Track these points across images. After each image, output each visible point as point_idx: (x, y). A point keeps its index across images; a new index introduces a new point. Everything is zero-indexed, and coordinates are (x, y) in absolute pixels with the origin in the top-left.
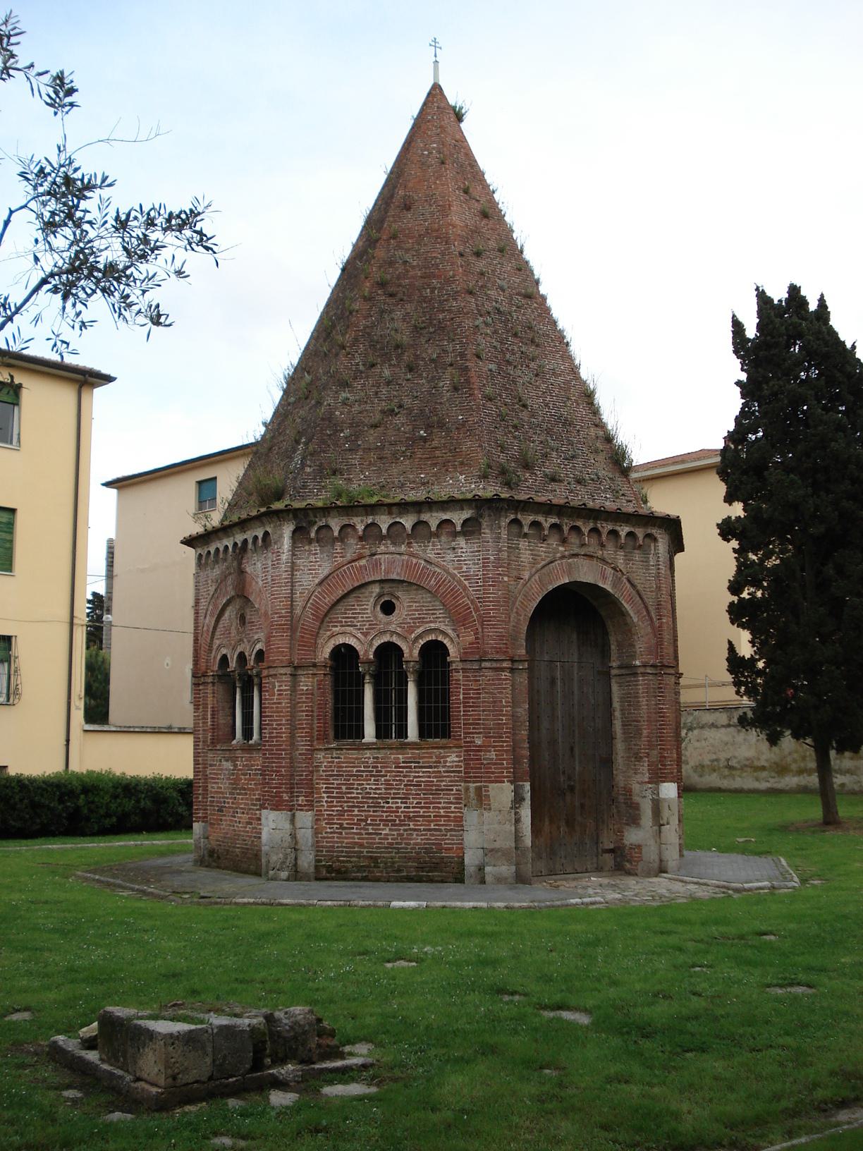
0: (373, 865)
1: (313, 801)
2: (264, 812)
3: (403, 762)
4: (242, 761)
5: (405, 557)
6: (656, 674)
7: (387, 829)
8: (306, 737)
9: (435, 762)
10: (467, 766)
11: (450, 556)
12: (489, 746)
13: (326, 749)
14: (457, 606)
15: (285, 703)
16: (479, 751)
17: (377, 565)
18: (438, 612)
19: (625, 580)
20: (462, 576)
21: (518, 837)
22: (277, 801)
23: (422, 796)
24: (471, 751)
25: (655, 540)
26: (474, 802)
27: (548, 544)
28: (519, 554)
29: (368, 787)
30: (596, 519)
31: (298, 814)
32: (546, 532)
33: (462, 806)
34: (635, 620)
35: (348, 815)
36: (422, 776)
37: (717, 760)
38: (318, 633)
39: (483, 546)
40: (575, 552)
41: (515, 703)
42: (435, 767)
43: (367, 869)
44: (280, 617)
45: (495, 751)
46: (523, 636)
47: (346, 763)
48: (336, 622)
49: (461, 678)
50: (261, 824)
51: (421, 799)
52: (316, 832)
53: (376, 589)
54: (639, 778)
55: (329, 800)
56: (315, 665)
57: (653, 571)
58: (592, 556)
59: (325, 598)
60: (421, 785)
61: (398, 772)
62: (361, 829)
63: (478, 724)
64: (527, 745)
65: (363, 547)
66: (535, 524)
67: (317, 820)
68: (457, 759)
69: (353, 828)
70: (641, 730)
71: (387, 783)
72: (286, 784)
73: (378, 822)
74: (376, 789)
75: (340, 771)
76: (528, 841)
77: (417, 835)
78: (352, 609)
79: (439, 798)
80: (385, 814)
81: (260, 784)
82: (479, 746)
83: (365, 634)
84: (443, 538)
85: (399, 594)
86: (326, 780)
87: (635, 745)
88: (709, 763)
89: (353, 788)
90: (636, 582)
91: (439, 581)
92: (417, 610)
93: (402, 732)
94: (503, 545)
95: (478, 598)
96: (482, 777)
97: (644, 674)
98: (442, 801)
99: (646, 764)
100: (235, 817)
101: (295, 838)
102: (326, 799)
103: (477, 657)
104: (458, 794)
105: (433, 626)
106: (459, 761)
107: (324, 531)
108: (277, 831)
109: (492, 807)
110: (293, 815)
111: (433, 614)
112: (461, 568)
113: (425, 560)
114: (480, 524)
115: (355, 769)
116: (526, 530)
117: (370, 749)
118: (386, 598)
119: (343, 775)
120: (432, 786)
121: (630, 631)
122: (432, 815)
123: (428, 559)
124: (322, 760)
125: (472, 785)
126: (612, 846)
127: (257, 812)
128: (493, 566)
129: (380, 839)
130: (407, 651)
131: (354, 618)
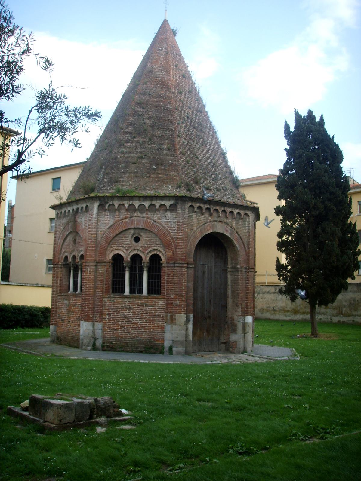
0: (126, 345)
1: (102, 318)
2: (82, 322)
4: (72, 300)
5: (145, 219)
7: (133, 331)
9: (154, 304)
10: (167, 306)
11: (164, 219)
12: (177, 299)
13: (109, 297)
15: (92, 277)
16: (172, 300)
17: (133, 221)
18: (158, 242)
19: (235, 232)
21: (187, 336)
22: (87, 318)
23: (148, 318)
25: (248, 216)
26: (169, 321)
28: (193, 219)
29: (125, 313)
30: (225, 206)
31: (96, 323)
32: (204, 211)
34: (239, 249)
36: (148, 310)
37: (269, 307)
38: (107, 249)
39: (178, 216)
41: (188, 281)
42: (154, 306)
46: (193, 253)
47: (116, 303)
49: (166, 270)
50: (80, 327)
51: (147, 319)
52: (103, 331)
53: (132, 232)
54: (237, 314)
56: (105, 262)
58: (222, 222)
59: (110, 234)
61: (139, 308)
62: (122, 330)
63: (173, 289)
64: (192, 299)
65: (127, 214)
66: (200, 208)
68: (163, 303)
70: (239, 294)
71: (134, 312)
72: (91, 311)
73: (129, 328)
76: (191, 338)
78: (121, 240)
80: (132, 325)
81: (80, 310)
82: (172, 298)
83: (127, 250)
84: (161, 212)
85: (142, 234)
86: (108, 310)
87: (236, 300)
88: (266, 308)
89: (119, 314)
90: (240, 233)
92: (149, 241)
93: (141, 291)
94: (186, 215)
95: (175, 237)
96: (173, 311)
97: (241, 271)
99: (240, 308)
100: (68, 323)
102: (108, 318)
103: (173, 262)
105: (155, 248)
106: (164, 304)
107: (111, 206)
108: (87, 330)
111: (156, 243)
112: (168, 224)
113: (153, 220)
114: (177, 206)
115: (120, 306)
116: (196, 210)
118: (136, 235)
119: (115, 308)
121: (236, 253)
122: (152, 326)
123: (154, 220)
124: (107, 302)
125: (169, 314)
126: (224, 341)
127: (79, 322)
128: (182, 224)
129: (130, 335)
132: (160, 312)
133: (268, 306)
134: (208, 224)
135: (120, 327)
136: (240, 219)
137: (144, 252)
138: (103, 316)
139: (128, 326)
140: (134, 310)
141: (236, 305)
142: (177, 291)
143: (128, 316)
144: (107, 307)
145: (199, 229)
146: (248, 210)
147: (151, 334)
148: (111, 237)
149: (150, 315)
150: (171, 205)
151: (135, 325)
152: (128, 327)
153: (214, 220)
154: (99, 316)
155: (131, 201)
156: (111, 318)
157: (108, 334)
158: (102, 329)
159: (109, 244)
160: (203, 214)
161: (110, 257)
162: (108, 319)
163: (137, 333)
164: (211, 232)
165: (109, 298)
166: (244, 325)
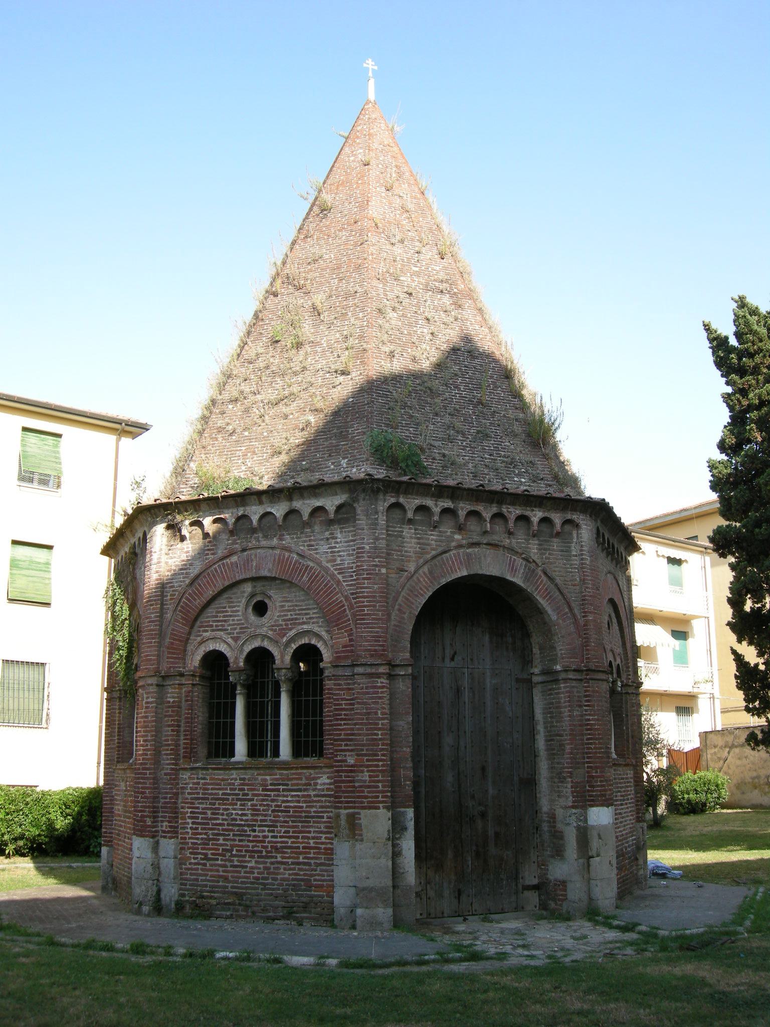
0: (237, 902)
1: (177, 827)
3: (271, 784)
5: (277, 552)
6: (581, 680)
8: (171, 754)
9: (306, 784)
11: (324, 548)
12: (361, 766)
13: (192, 769)
14: (330, 604)
16: (351, 771)
17: (248, 561)
18: (311, 612)
19: (540, 573)
20: (336, 570)
21: (396, 872)
22: (142, 826)
23: (290, 823)
24: (342, 771)
25: (577, 526)
26: (346, 832)
27: (440, 532)
28: (403, 542)
29: (234, 812)
30: (500, 503)
31: (163, 842)
32: (436, 518)
33: (332, 835)
34: (554, 617)
35: (213, 844)
36: (290, 800)
37: (758, 777)
38: (188, 639)
40: (474, 541)
41: (393, 714)
42: (305, 790)
43: (231, 907)
44: (150, 622)
45: (368, 771)
46: (407, 637)
47: (212, 784)
48: (207, 626)
51: (288, 827)
52: (181, 862)
54: (562, 802)
55: (194, 826)
56: (182, 675)
57: (576, 561)
59: (195, 600)
60: (289, 812)
61: (266, 795)
62: (225, 860)
65: (234, 543)
67: (182, 849)
68: (328, 781)
69: (217, 859)
70: (563, 745)
71: (254, 809)
72: (149, 807)
73: (243, 853)
74: (242, 815)
75: (205, 794)
77: (285, 869)
78: (223, 612)
79: (307, 827)
80: (251, 844)
82: (352, 766)
83: (236, 639)
84: (317, 528)
85: (271, 593)
87: (558, 763)
88: (751, 780)
89: (218, 814)
90: (554, 575)
91: (312, 576)
92: (289, 611)
94: (381, 533)
95: (352, 594)
96: (355, 802)
97: (566, 680)
98: (312, 830)
99: (569, 785)
101: (159, 868)
102: (191, 825)
103: (349, 662)
104: (329, 822)
105: (305, 627)
106: (330, 784)
108: (141, 860)
109: (365, 838)
110: (157, 843)
111: (306, 614)
112: (335, 561)
113: (298, 554)
114: (354, 509)
115: (221, 792)
116: (410, 515)
117: (236, 769)
118: (259, 598)
119: (208, 799)
120: (301, 812)
121: (550, 631)
122: (301, 846)
123: (300, 552)
124: (188, 781)
125: (344, 812)
126: (535, 881)
128: (369, 557)
129: (245, 872)
130: (279, 657)
131: (225, 621)
132: (322, 807)
133: (755, 774)
134: (451, 553)
135: (220, 852)
136: (552, 536)
137: (277, 642)
138: (180, 821)
139: (242, 846)
140: (255, 802)
141: (560, 778)
142: (363, 745)
143: (241, 820)
144: (189, 796)
145: (426, 569)
146: (574, 510)
147: (300, 869)
148: (196, 607)
149: (295, 817)
150: (339, 508)
151: (260, 844)
152: (241, 851)
154: (169, 822)
155: (242, 508)
156: (200, 826)
157: (192, 869)
158: (175, 857)
159: (192, 627)
160: (435, 527)
161: (195, 660)
162: (191, 828)
163: (265, 868)
164: (465, 573)
165: (194, 772)
166: (584, 835)
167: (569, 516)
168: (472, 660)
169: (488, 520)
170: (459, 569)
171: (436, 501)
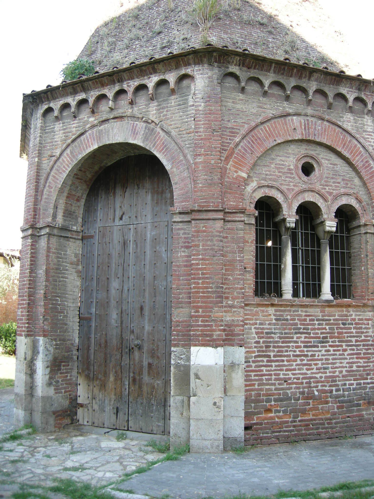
19: (158, 130)
28: (54, 136)
40: (104, 118)
58: (122, 117)
134: (87, 134)
153: (101, 119)
160: (75, 117)
164: (96, 147)
167: (183, 71)
168: (136, 217)
169: (111, 98)
170: (92, 144)
171: (74, 97)
